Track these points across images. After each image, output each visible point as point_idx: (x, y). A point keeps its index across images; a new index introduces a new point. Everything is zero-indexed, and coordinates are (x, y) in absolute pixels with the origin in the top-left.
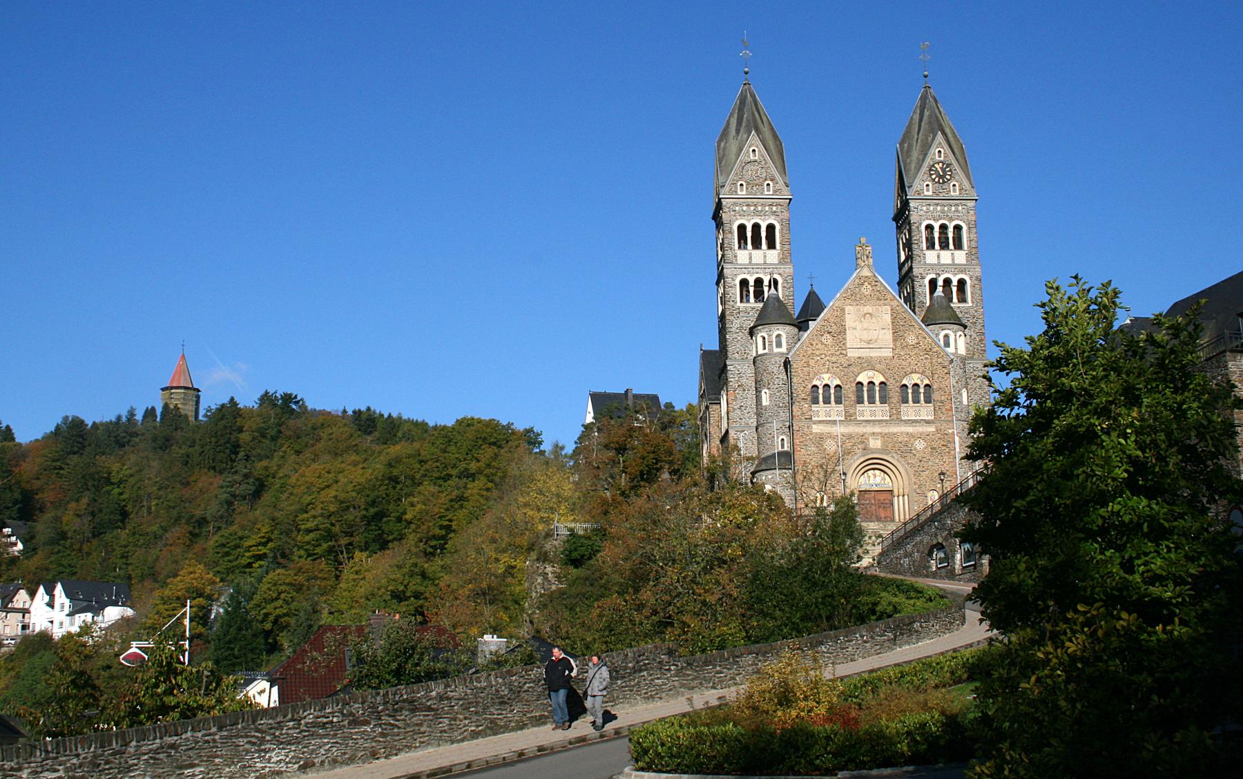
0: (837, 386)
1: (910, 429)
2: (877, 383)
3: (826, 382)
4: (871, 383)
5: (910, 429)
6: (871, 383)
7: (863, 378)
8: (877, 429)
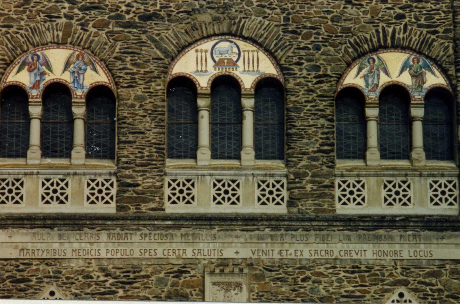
0: (99, 96)
1: (366, 251)
2: (248, 82)
3: (58, 73)
4: (226, 85)
5: (366, 251)
6: (226, 85)
7: (197, 65)
8: (238, 248)
